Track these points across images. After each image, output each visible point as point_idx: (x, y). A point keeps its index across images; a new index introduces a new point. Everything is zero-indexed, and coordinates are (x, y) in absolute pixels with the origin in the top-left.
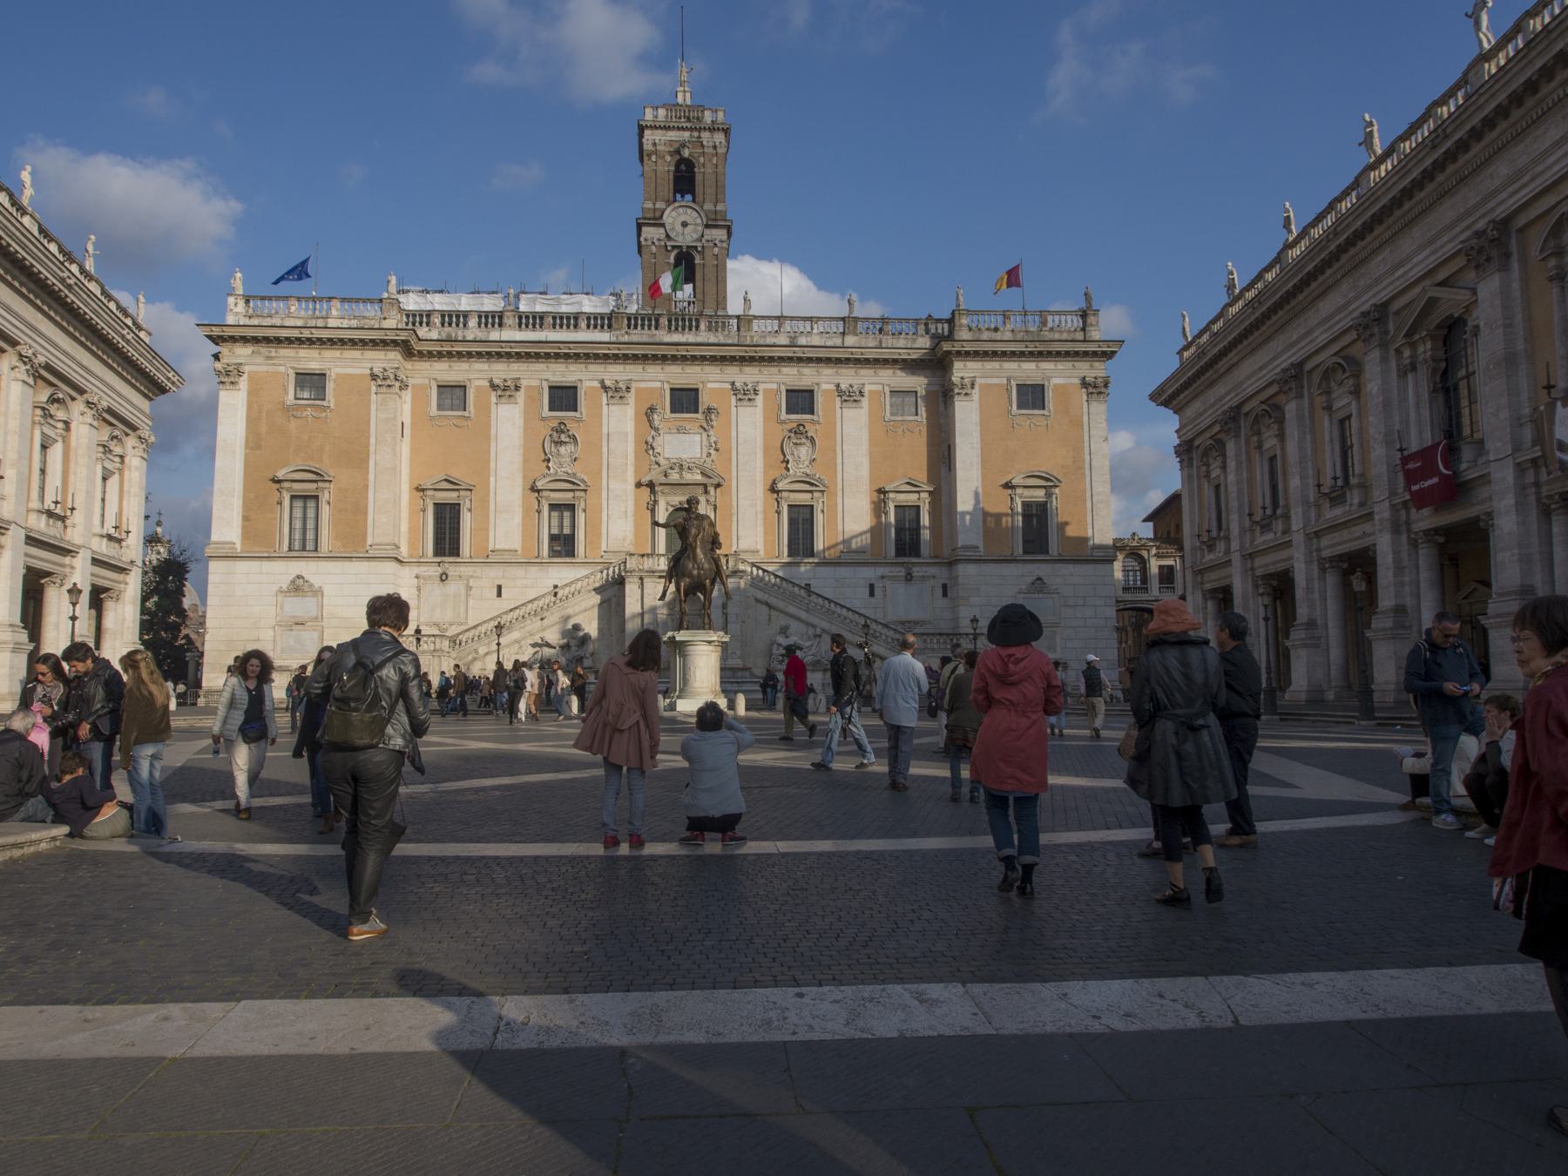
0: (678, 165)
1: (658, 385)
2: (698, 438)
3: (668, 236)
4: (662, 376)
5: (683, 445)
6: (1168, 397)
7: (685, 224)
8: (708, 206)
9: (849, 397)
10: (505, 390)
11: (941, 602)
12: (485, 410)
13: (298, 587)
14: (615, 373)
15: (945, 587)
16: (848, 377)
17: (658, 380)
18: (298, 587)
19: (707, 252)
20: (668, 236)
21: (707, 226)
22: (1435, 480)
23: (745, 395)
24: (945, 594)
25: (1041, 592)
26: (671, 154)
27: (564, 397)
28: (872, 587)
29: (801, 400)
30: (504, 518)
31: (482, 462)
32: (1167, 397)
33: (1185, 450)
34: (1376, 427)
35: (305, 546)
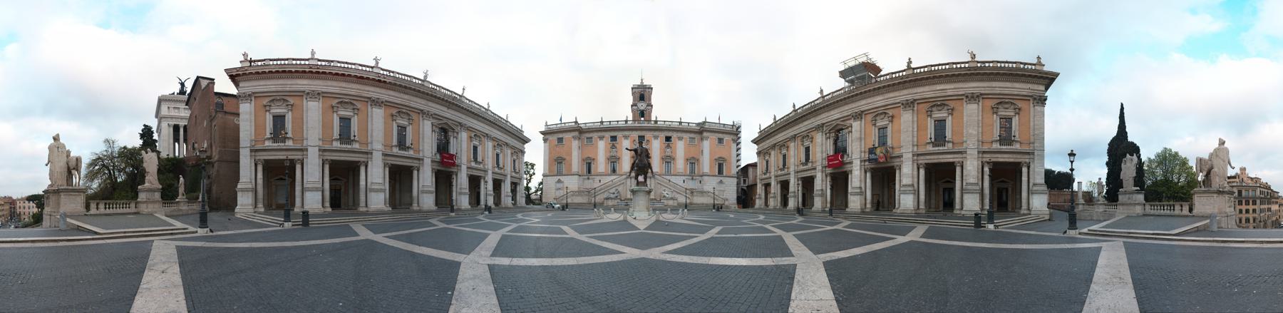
6: (755, 141)
9: (680, 139)
10: (601, 138)
13: (559, 181)
14: (627, 133)
16: (680, 134)
17: (635, 135)
18: (559, 181)
23: (656, 137)
27: (614, 138)
29: (668, 139)
30: (601, 165)
31: (596, 154)
32: (755, 141)
33: (759, 153)
34: (818, 149)
35: (560, 173)
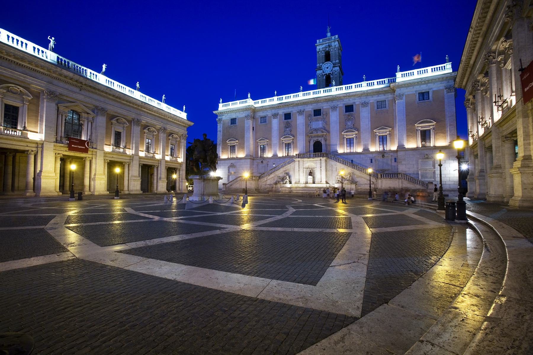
2: (321, 122)
3: (323, 72)
4: (311, 107)
5: (318, 124)
7: (327, 68)
8: (334, 62)
11: (394, 164)
12: (271, 123)
15: (395, 159)
19: (334, 74)
20: (323, 72)
21: (333, 67)
24: (395, 161)
25: (427, 158)
28: (371, 160)
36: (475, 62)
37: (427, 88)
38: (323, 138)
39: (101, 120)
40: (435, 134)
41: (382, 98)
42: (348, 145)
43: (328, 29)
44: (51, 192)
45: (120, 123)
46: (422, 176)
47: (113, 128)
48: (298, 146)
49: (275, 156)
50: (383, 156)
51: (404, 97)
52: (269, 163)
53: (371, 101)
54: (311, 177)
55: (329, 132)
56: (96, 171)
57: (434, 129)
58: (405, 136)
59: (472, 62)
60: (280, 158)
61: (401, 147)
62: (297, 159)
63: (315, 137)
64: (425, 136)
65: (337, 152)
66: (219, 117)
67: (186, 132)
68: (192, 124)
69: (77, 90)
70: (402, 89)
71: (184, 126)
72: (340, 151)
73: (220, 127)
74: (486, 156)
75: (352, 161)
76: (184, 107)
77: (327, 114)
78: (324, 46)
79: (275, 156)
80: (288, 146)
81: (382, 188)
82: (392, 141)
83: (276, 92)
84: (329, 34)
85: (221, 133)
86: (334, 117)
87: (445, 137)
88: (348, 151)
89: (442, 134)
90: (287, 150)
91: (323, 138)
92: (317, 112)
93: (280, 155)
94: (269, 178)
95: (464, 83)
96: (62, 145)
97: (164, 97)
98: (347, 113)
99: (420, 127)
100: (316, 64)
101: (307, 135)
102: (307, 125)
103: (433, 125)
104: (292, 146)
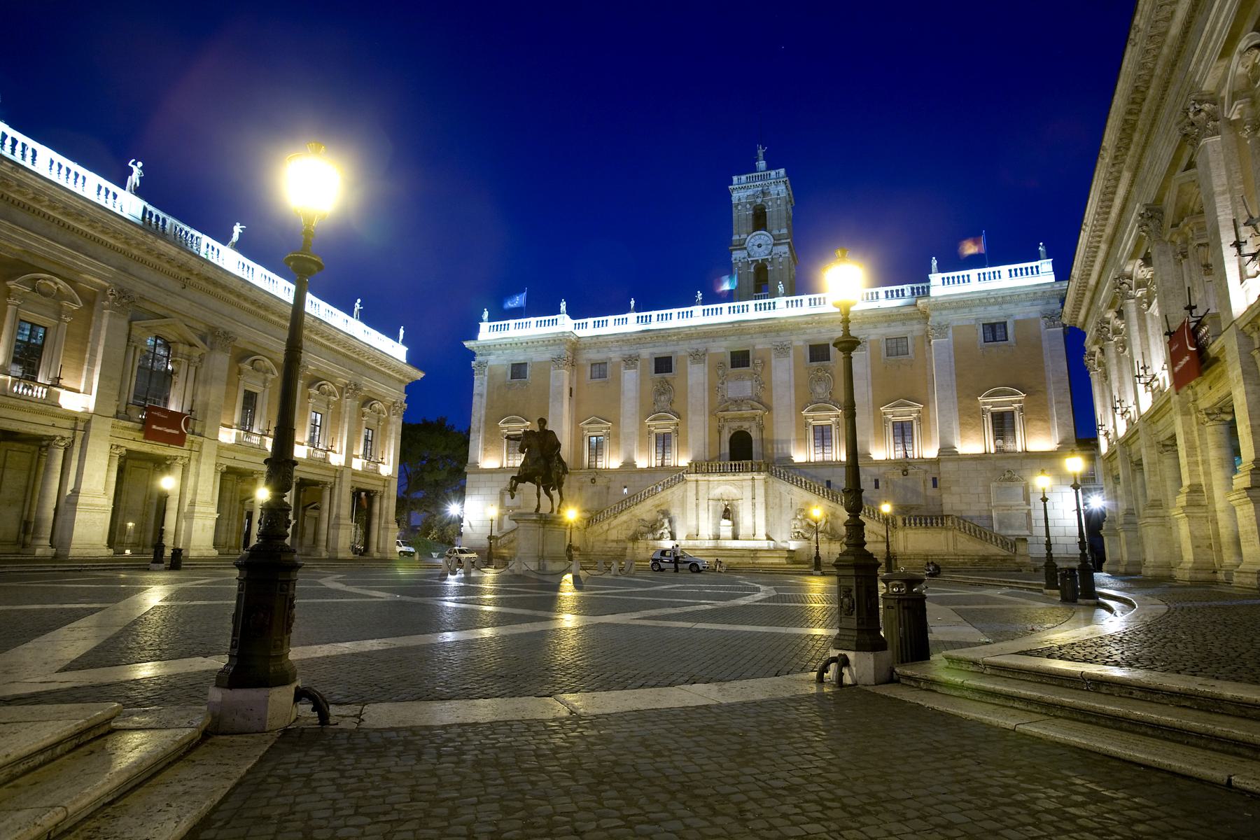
0: (755, 209)
1: (723, 350)
2: (749, 383)
3: (749, 255)
4: (725, 344)
5: (741, 386)
7: (760, 246)
8: (775, 232)
11: (931, 492)
15: (934, 480)
20: (749, 255)
22: (1187, 358)
24: (935, 485)
25: (1010, 479)
26: (750, 203)
28: (877, 482)
36: (1098, 283)
37: (1002, 313)
38: (753, 424)
39: (221, 361)
40: (1026, 422)
41: (897, 330)
42: (818, 443)
43: (761, 152)
44: (93, 546)
45: (258, 371)
46: (1001, 523)
47: (242, 383)
48: (690, 441)
49: (629, 465)
50: (905, 472)
51: (950, 331)
52: (611, 485)
53: (872, 337)
54: (729, 523)
55: (769, 408)
56: (195, 493)
57: (1021, 409)
58: (955, 425)
59: (1092, 281)
60: (642, 470)
61: (947, 451)
62: (693, 477)
63: (733, 419)
64: (1003, 425)
65: (789, 458)
66: (478, 358)
67: (404, 397)
68: (419, 375)
69: (176, 286)
70: (944, 312)
71: (401, 381)
72: (799, 456)
73: (480, 385)
74: (1134, 480)
75: (829, 483)
76: (402, 332)
77: (765, 363)
78: (750, 192)
79: (629, 465)
80: (664, 442)
81: (908, 552)
82: (926, 436)
83: (633, 303)
84: (762, 164)
85: (484, 401)
86: (783, 375)
87: (1048, 431)
88: (819, 458)
89: (1040, 424)
90: (660, 450)
91: (753, 424)
92: (740, 359)
93: (642, 462)
94: (615, 522)
95: (1081, 318)
96: (130, 424)
97: (357, 306)
98: (815, 364)
99: (990, 403)
100: (731, 235)
101: (712, 413)
102: (714, 389)
103: (1020, 402)
104: (674, 442)
